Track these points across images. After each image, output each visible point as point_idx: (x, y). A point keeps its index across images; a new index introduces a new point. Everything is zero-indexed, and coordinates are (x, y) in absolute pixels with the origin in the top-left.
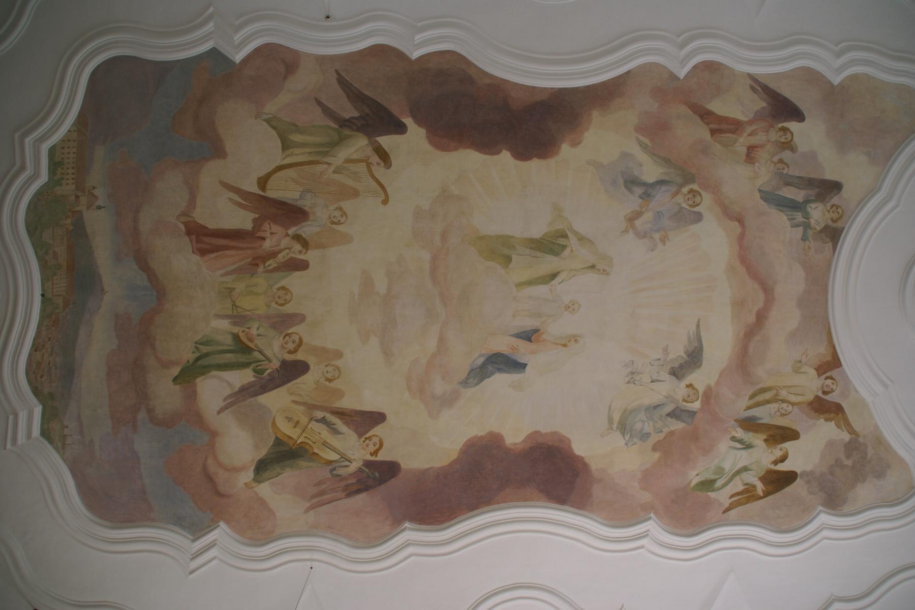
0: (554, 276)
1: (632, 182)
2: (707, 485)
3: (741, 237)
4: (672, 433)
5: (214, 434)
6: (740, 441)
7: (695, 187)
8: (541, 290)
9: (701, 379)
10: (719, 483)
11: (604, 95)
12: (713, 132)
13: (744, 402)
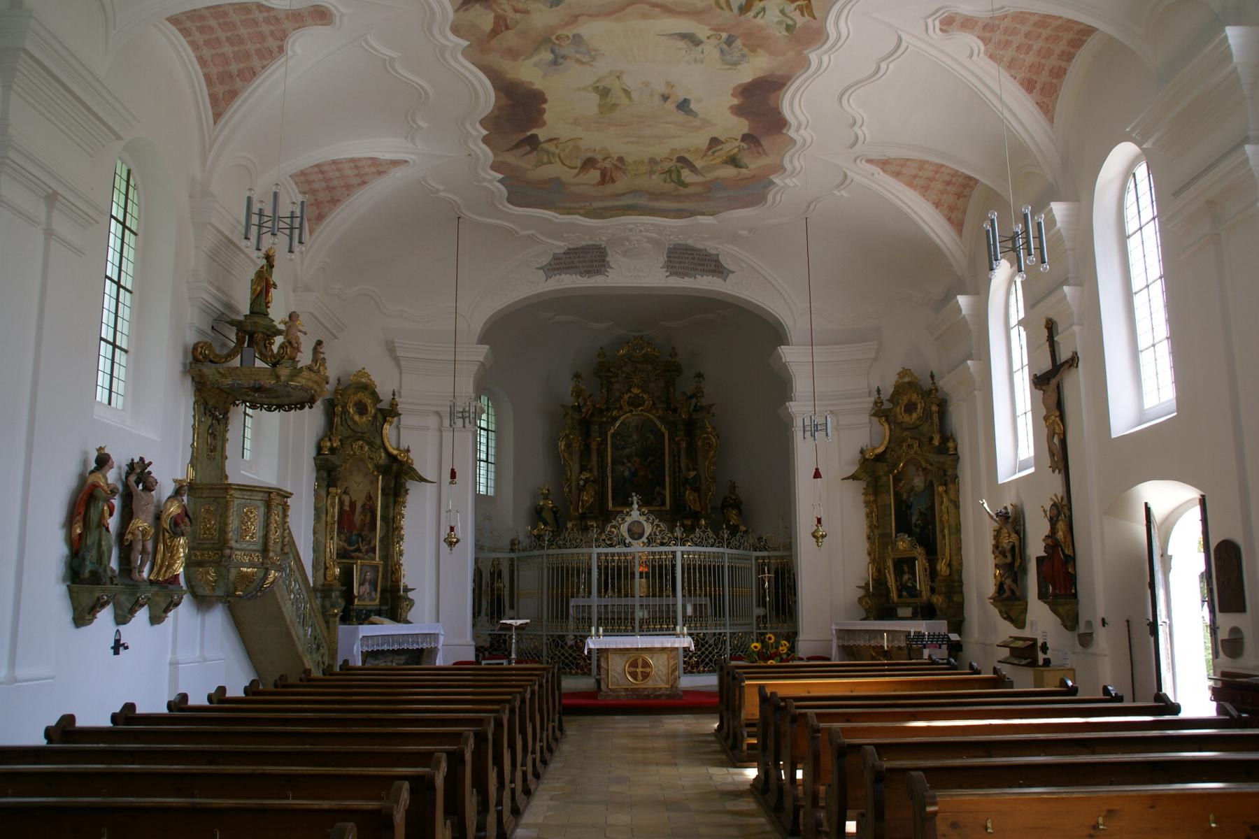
0: (625, 91)
1: (555, 63)
2: (789, 28)
3: (590, 15)
4: (744, 45)
5: (717, 178)
6: (758, 14)
7: (553, 38)
8: (634, 95)
9: (702, 31)
10: (790, 22)
11: (493, 75)
12: (507, 28)
13: (727, 13)
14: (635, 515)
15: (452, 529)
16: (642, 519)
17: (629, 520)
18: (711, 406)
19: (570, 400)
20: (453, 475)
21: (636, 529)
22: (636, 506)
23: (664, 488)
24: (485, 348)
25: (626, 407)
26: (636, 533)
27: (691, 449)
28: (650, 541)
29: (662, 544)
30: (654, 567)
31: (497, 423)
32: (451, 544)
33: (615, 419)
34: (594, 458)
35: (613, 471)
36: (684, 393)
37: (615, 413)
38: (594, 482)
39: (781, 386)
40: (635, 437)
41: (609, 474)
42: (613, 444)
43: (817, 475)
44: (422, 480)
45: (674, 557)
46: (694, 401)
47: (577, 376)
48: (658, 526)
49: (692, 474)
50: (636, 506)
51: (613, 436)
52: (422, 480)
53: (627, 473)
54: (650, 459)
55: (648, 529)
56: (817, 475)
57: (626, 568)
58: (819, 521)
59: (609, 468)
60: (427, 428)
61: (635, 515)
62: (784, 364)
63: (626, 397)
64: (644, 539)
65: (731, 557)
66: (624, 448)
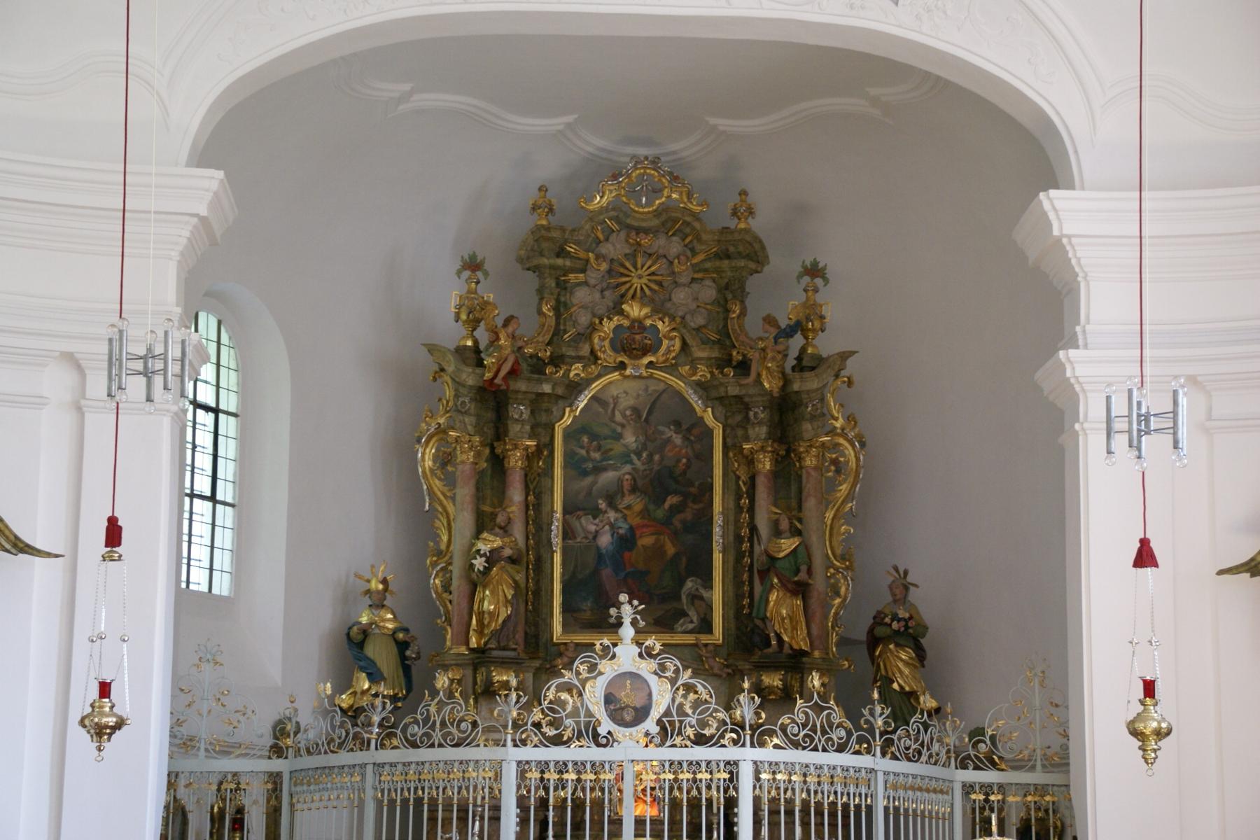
14: (627, 656)
15: (105, 689)
16: (646, 668)
17: (608, 669)
18: (845, 356)
19: (453, 334)
20: (114, 534)
21: (627, 696)
22: (627, 632)
23: (708, 585)
24: (213, 178)
25: (608, 356)
26: (627, 711)
27: (787, 474)
28: (667, 731)
29: (700, 740)
30: (675, 805)
31: (244, 391)
32: (101, 732)
33: (575, 388)
34: (516, 494)
35: (568, 533)
36: (770, 320)
37: (576, 370)
38: (513, 560)
39: (1045, 304)
40: (630, 439)
41: (557, 541)
42: (569, 457)
43: (1145, 557)
44: (21, 547)
45: (733, 778)
46: (797, 341)
47: (473, 265)
48: (689, 688)
49: (788, 545)
50: (627, 632)
51: (569, 435)
52: (21, 547)
53: (605, 540)
54: (672, 500)
55: (662, 697)
56: (1145, 557)
57: (598, 805)
58: (1149, 688)
59: (556, 527)
60: (38, 402)
61: (627, 656)
62: (1058, 246)
63: (608, 326)
64: (650, 725)
65: (894, 783)
66: (598, 470)
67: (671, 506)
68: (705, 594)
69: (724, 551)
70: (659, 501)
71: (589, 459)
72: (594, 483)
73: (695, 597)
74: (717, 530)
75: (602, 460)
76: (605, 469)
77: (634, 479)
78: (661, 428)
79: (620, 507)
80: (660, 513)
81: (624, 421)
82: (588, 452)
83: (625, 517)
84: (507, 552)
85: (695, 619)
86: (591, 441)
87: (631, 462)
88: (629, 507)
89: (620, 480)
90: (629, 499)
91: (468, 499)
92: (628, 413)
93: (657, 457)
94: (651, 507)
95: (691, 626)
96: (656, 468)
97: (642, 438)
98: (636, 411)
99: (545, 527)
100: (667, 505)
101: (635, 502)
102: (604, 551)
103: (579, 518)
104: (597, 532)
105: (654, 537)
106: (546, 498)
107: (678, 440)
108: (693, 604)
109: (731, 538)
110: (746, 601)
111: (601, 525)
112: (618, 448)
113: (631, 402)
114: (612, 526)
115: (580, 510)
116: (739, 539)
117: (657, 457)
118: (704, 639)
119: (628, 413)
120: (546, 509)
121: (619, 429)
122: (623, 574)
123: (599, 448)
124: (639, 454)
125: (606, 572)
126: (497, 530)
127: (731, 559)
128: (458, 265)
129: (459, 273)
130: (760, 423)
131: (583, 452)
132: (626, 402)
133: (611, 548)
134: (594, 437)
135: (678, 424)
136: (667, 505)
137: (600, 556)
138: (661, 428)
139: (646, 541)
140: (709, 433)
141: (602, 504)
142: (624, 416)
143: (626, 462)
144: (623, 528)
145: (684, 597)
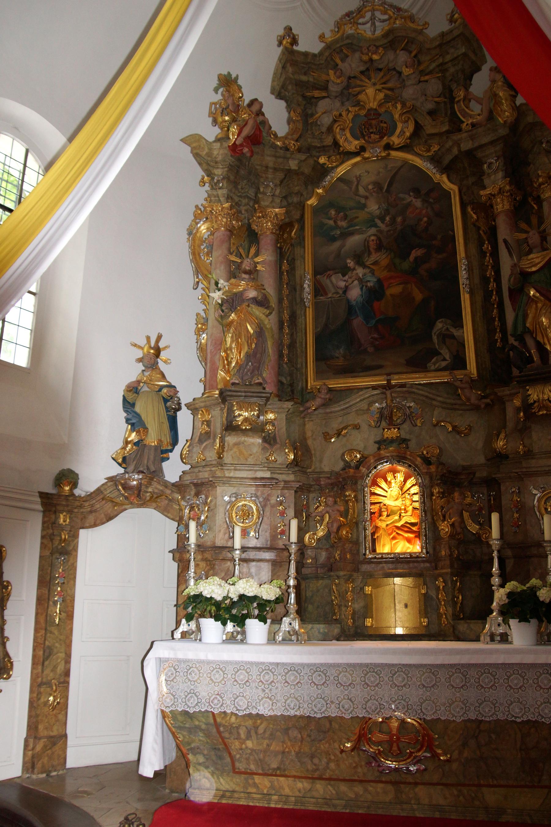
23: (458, 323)
35: (319, 290)
40: (373, 207)
51: (316, 210)
53: (355, 293)
54: (415, 253)
59: (307, 286)
66: (345, 235)
67: (416, 258)
68: (456, 332)
69: (472, 293)
70: (405, 256)
71: (337, 227)
72: (343, 246)
73: (445, 337)
74: (463, 275)
75: (349, 227)
76: (352, 234)
77: (379, 239)
78: (401, 195)
79: (368, 263)
80: (406, 265)
81: (367, 194)
82: (335, 222)
83: (373, 272)
84: (252, 294)
85: (447, 357)
86: (338, 212)
87: (376, 226)
88: (376, 263)
89: (366, 241)
90: (374, 257)
91: (221, 259)
92: (370, 187)
93: (399, 219)
94: (397, 261)
95: (444, 364)
96: (399, 228)
97: (384, 206)
98: (378, 185)
99: (298, 288)
100: (412, 258)
101: (383, 258)
102: (354, 303)
103: (329, 277)
104: (347, 287)
105: (402, 286)
106: (298, 263)
107: (418, 203)
108: (444, 343)
109: (477, 280)
110: (498, 336)
111: (350, 281)
112: (362, 215)
113: (372, 178)
114: (361, 281)
115: (330, 270)
116: (485, 280)
117: (399, 219)
118: (459, 374)
119: (370, 187)
120: (298, 273)
121: (363, 201)
122: (374, 322)
123: (345, 217)
124: (382, 218)
125: (358, 322)
126: (244, 276)
127: (479, 298)
128: (215, 82)
129: (216, 90)
130: (496, 172)
131: (331, 222)
132: (367, 179)
133: (360, 299)
134: (340, 209)
135: (417, 192)
136: (412, 258)
137: (350, 309)
138: (401, 195)
139: (394, 290)
140: (447, 195)
141: (351, 263)
142: (366, 189)
143: (371, 226)
144: (372, 281)
145: (435, 338)
